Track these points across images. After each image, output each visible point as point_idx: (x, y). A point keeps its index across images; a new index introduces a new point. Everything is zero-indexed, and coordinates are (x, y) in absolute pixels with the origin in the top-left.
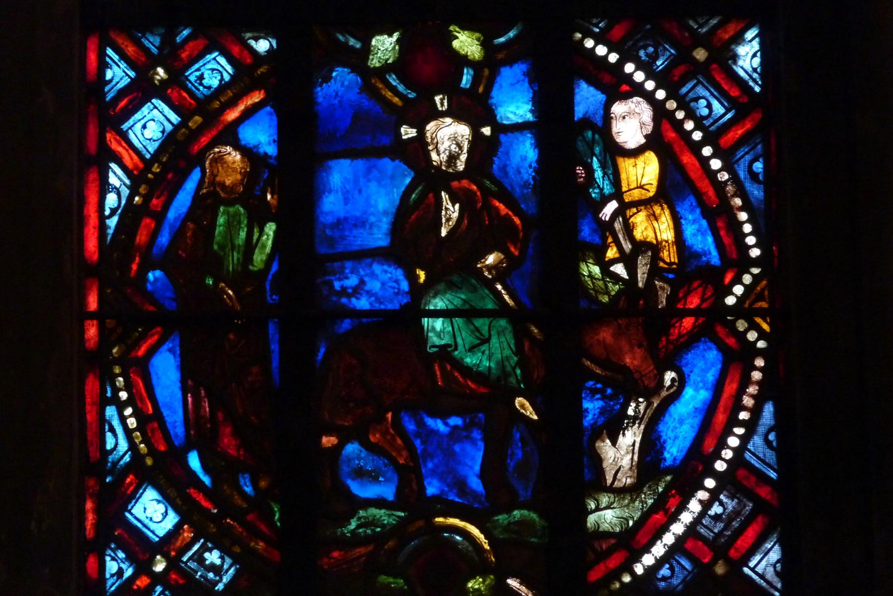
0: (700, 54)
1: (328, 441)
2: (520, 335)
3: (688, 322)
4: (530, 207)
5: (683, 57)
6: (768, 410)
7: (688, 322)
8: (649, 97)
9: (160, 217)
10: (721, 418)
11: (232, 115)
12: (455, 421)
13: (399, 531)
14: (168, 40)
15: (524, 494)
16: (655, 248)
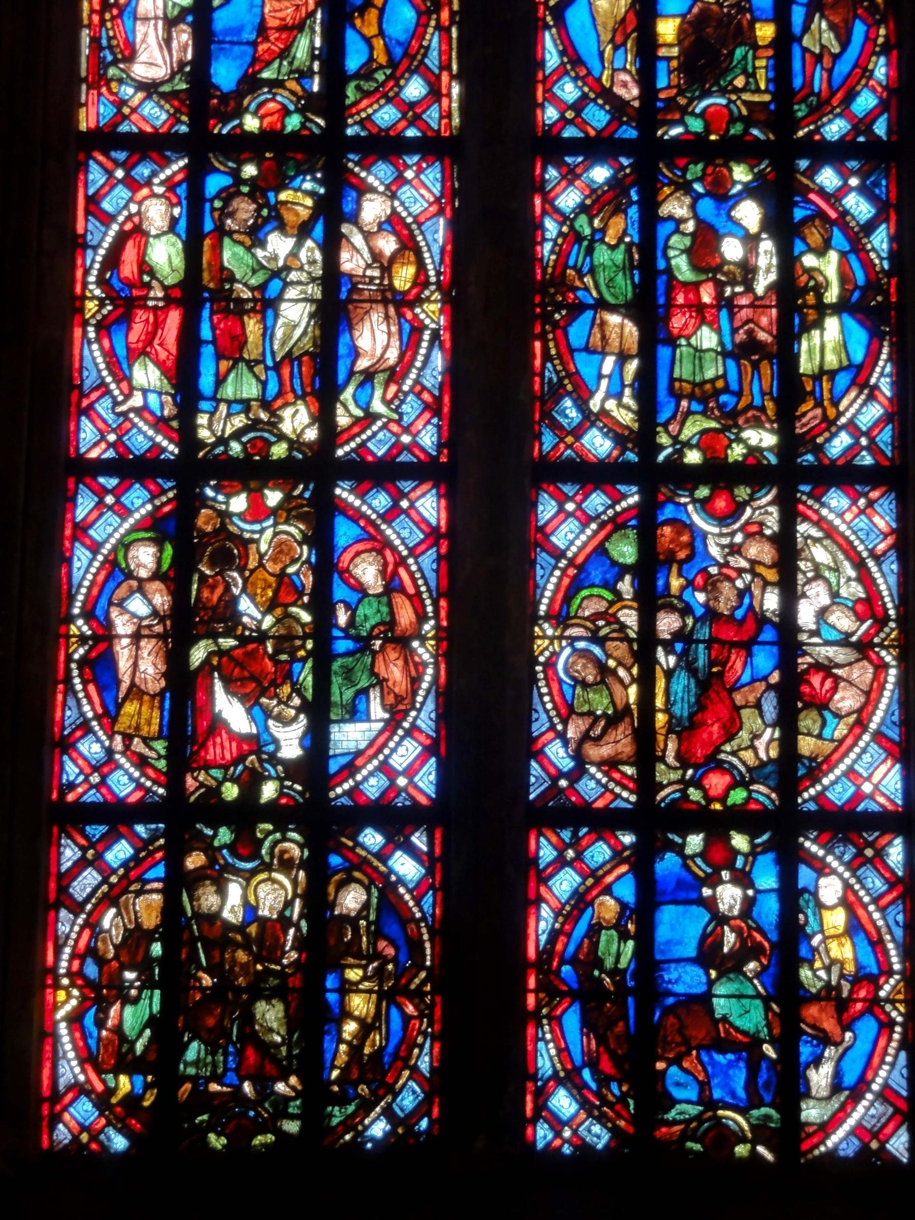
0: (869, 852)
1: (660, 1065)
2: (767, 1009)
3: (859, 1006)
4: (774, 936)
5: (860, 854)
6: (903, 1055)
7: (859, 1006)
8: (840, 876)
9: (569, 935)
10: (876, 1060)
11: (609, 879)
12: (730, 1057)
13: (699, 1118)
14: (575, 834)
15: (767, 1098)
16: (842, 963)
